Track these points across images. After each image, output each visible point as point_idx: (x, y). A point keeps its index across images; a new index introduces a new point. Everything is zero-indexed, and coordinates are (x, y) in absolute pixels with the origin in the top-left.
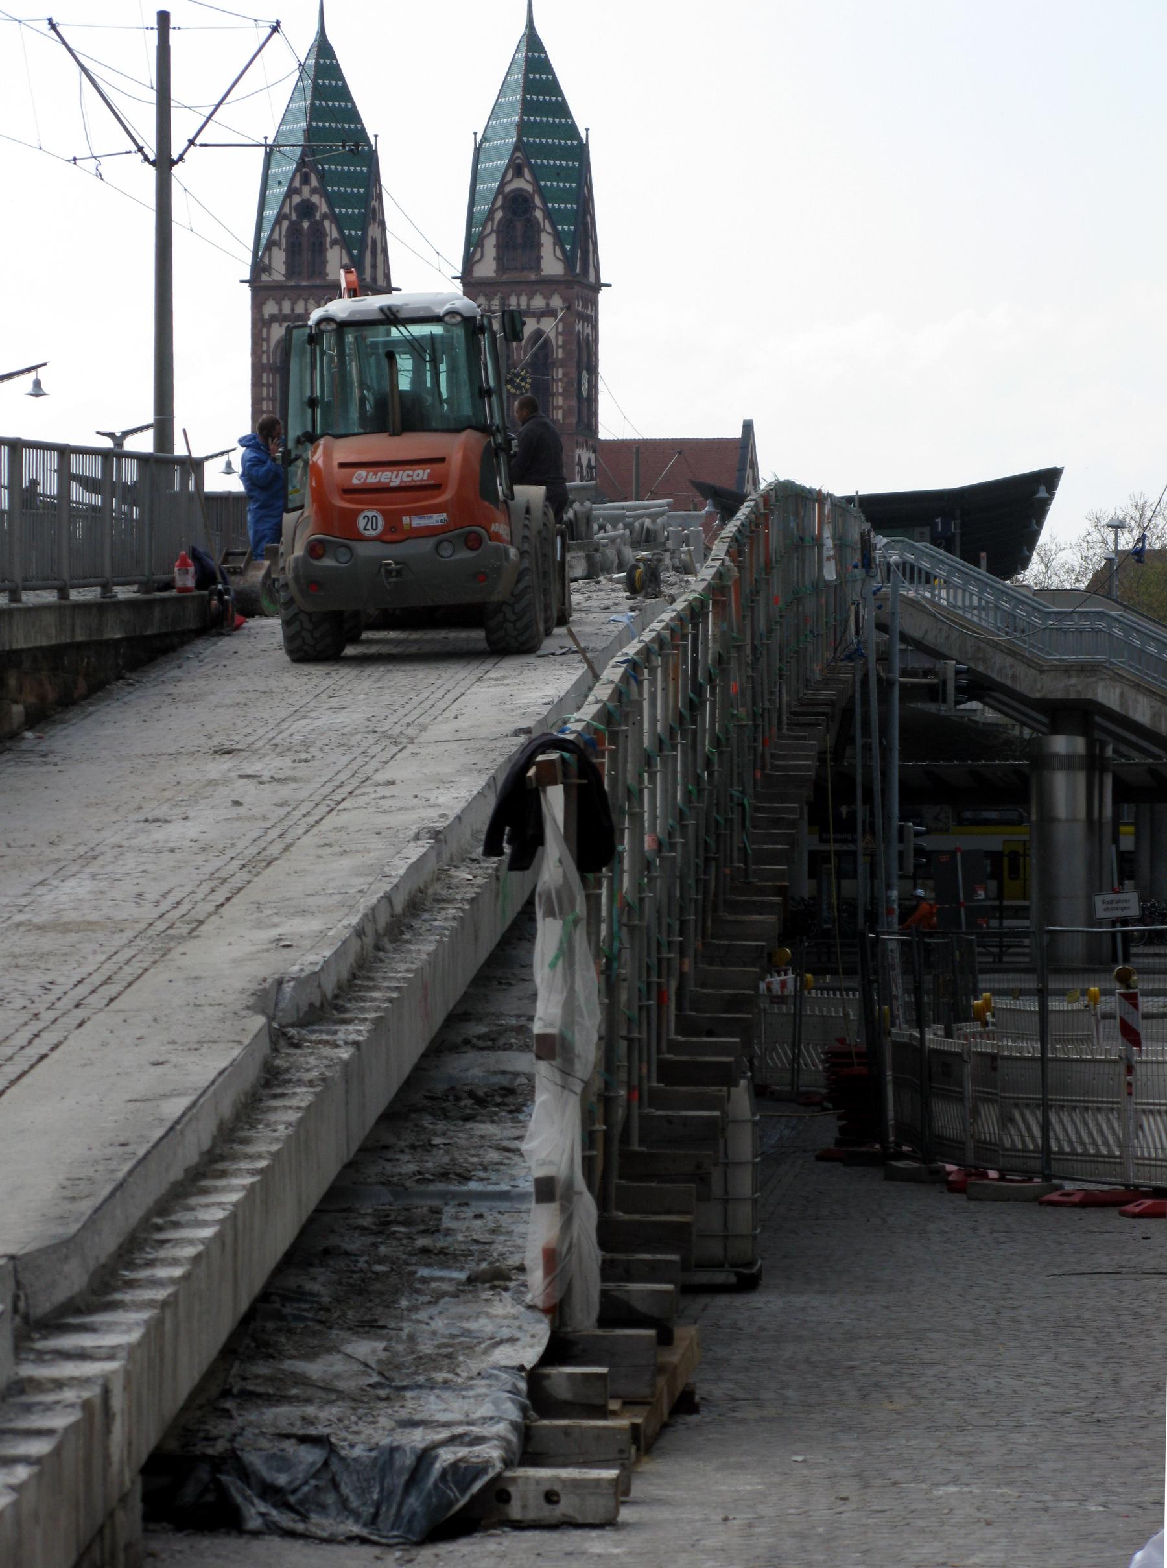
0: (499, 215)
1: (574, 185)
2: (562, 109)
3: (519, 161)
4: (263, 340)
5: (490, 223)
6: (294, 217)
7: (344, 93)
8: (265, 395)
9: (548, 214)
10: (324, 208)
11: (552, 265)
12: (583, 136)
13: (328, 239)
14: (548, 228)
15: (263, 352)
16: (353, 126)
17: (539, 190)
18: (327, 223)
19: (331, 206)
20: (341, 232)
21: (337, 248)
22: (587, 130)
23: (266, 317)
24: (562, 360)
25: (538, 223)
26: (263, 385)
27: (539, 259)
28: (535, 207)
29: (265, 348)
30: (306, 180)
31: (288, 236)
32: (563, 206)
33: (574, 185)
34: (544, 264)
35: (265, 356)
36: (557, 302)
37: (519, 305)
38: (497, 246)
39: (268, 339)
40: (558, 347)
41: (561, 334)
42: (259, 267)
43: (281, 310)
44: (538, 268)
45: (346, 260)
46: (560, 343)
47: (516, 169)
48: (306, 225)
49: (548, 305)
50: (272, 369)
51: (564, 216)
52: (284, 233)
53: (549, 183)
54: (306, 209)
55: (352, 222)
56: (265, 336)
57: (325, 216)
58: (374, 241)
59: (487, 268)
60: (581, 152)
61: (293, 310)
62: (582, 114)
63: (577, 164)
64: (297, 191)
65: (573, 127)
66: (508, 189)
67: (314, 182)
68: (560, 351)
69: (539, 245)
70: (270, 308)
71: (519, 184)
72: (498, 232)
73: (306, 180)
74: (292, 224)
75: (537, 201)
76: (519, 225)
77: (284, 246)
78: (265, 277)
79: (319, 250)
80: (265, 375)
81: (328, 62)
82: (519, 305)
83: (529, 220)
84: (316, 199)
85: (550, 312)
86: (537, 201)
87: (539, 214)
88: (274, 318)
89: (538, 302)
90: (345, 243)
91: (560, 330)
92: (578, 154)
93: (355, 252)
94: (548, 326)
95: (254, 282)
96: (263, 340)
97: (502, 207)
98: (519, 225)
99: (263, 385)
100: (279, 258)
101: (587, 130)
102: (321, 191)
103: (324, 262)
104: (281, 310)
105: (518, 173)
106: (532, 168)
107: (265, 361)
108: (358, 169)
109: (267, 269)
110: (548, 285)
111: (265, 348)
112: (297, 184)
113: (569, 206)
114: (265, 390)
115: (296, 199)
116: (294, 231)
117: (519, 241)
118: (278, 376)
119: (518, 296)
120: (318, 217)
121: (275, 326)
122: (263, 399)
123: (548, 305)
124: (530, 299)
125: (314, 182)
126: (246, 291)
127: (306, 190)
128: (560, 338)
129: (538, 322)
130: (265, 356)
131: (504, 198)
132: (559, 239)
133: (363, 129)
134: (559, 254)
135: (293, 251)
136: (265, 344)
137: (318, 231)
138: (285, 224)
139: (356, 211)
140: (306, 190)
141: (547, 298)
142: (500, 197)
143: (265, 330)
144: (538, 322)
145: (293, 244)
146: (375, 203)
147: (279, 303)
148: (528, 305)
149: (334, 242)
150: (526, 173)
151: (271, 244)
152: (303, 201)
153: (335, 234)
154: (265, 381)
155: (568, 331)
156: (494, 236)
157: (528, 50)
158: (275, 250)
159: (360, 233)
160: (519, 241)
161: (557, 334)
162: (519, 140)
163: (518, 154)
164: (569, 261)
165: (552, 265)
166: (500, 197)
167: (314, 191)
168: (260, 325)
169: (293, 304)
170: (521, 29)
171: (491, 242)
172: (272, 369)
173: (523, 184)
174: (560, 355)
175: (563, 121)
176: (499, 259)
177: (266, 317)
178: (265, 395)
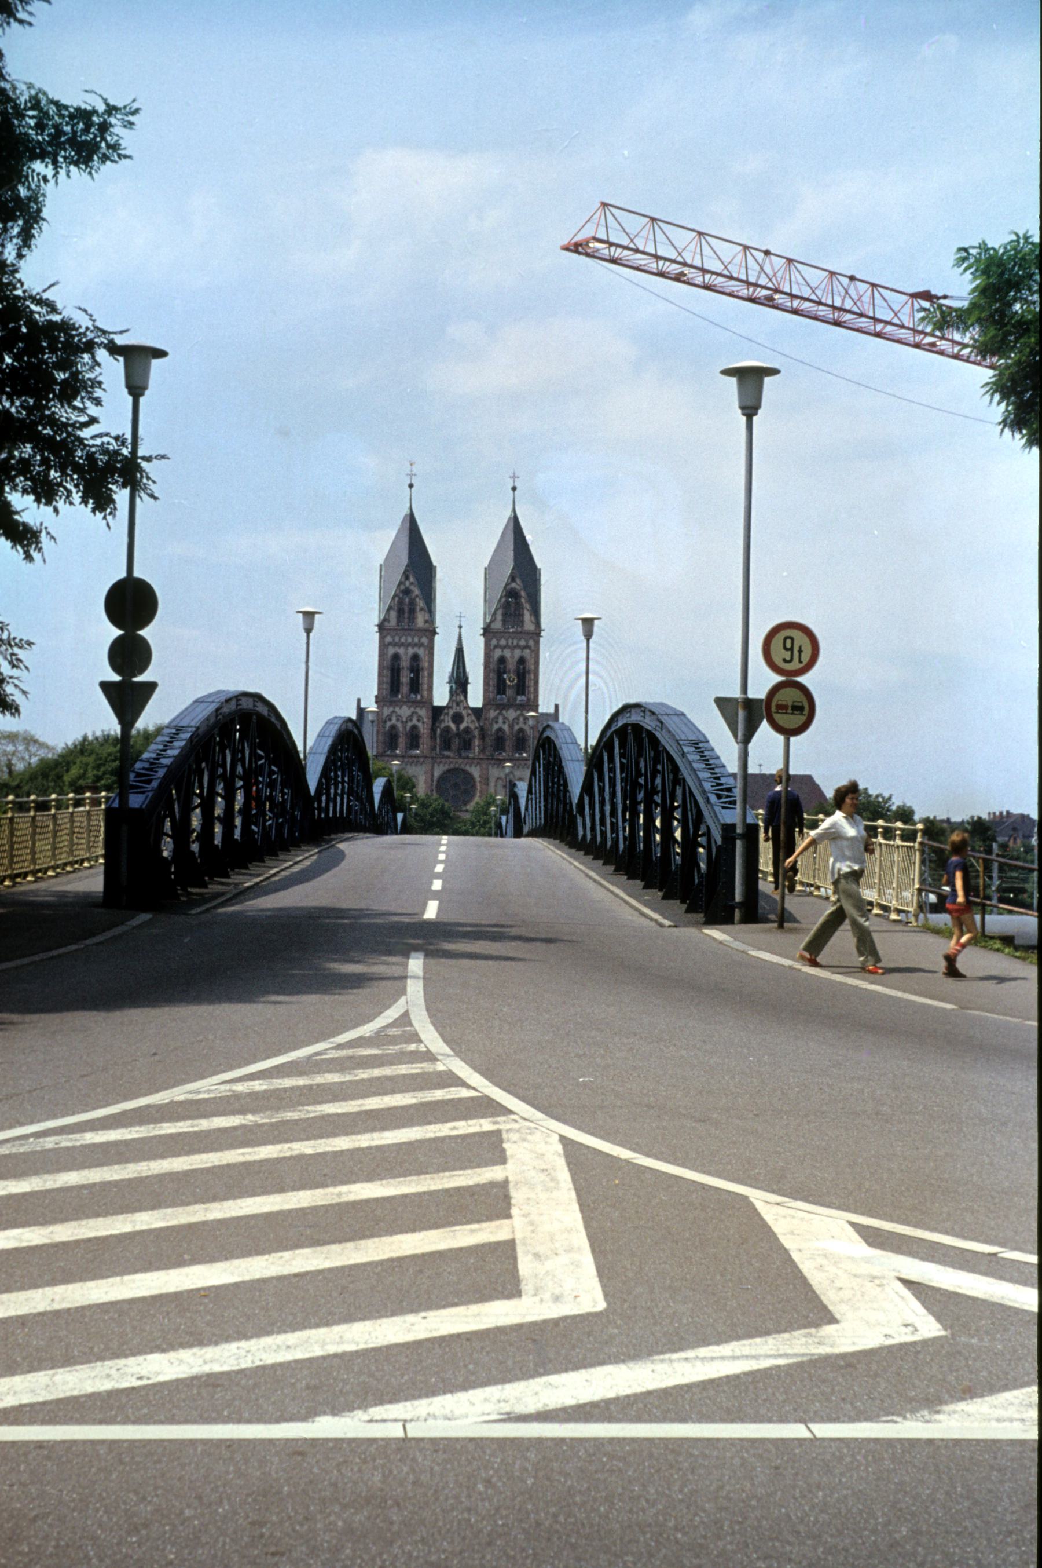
0: (503, 600)
13: (418, 608)
27: (523, 622)
30: (407, 578)
36: (531, 643)
44: (522, 626)
47: (513, 578)
48: (407, 600)
54: (407, 592)
66: (509, 587)
69: (523, 615)
70: (388, 639)
71: (513, 585)
73: (407, 578)
78: (386, 624)
79: (412, 611)
84: (412, 587)
87: (523, 600)
88: (390, 644)
89: (522, 643)
95: (381, 627)
100: (393, 614)
109: (389, 621)
110: (528, 633)
115: (402, 587)
116: (401, 602)
120: (413, 596)
125: (412, 579)
127: (407, 583)
135: (400, 612)
137: (412, 603)
140: (407, 583)
149: (422, 609)
150: (518, 581)
151: (390, 608)
165: (529, 626)
171: (500, 612)
173: (517, 585)
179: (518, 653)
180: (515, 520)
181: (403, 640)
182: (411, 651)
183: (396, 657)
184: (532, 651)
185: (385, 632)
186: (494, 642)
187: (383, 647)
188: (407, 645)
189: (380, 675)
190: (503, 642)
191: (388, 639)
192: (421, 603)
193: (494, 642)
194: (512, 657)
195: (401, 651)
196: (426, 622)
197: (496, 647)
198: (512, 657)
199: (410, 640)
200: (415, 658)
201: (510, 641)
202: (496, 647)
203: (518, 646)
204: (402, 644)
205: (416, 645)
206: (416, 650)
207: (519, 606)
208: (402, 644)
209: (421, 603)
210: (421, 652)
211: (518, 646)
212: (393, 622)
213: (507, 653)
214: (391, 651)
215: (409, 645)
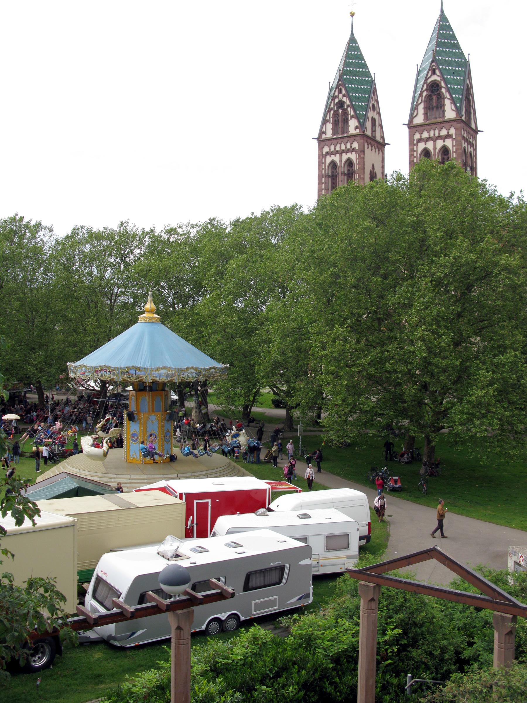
0: (425, 93)
1: (462, 78)
2: (457, 46)
3: (434, 67)
4: (323, 163)
5: (421, 98)
6: (336, 109)
7: (361, 57)
8: (323, 188)
9: (448, 90)
10: (348, 103)
11: (450, 113)
12: (467, 58)
13: (350, 116)
14: (448, 96)
15: (323, 169)
16: (364, 70)
17: (444, 79)
18: (349, 109)
19: (351, 101)
20: (355, 111)
21: (353, 119)
22: (469, 54)
23: (324, 153)
24: (456, 158)
25: (443, 94)
26: (323, 183)
27: (444, 111)
28: (442, 87)
29: (323, 167)
30: (340, 92)
31: (333, 117)
32: (456, 87)
34: (446, 114)
35: (323, 171)
36: (452, 131)
37: (434, 134)
38: (425, 108)
39: (325, 163)
40: (453, 152)
41: (455, 146)
42: (322, 133)
43: (330, 150)
44: (444, 116)
45: (357, 124)
46: (454, 150)
48: (340, 111)
49: (448, 133)
50: (328, 176)
51: (457, 91)
52: (331, 116)
53: (449, 77)
54: (341, 104)
55: (361, 108)
56: (323, 161)
57: (348, 106)
58: (373, 120)
59: (419, 119)
60: (466, 64)
61: (335, 149)
62: (467, 46)
63: (463, 69)
64: (337, 97)
65: (462, 54)
66: (429, 81)
67: (344, 92)
68: (454, 154)
69: (444, 105)
70: (326, 149)
71: (434, 78)
72: (425, 101)
73: (340, 92)
74: (335, 111)
75: (443, 84)
76: (434, 97)
77: (331, 122)
78: (324, 136)
79: (346, 122)
80: (323, 179)
81: (354, 45)
82: (434, 134)
83: (439, 94)
84: (345, 99)
85: (448, 136)
86: (443, 84)
87: (443, 90)
88: (327, 153)
89: (444, 132)
90: (357, 117)
91: (454, 144)
92: (463, 67)
93: (361, 120)
94: (449, 143)
96: (323, 163)
97: (426, 90)
98: (434, 97)
99: (323, 183)
100: (329, 127)
101: (469, 54)
102: (347, 95)
103: (349, 126)
104: (330, 150)
105: (434, 73)
107: (323, 173)
108: (366, 87)
109: (324, 133)
111: (323, 167)
112: (336, 94)
113: (459, 87)
114: (323, 185)
115: (337, 100)
116: (336, 114)
117: (435, 105)
118: (330, 179)
119: (434, 130)
122: (322, 189)
123: (448, 133)
124: (440, 131)
125: (344, 92)
126: (316, 142)
127: (340, 96)
128: (454, 148)
129: (444, 142)
130: (323, 171)
131: (427, 85)
132: (453, 101)
133: (369, 71)
134: (453, 108)
135: (335, 124)
136: (323, 165)
137: (345, 113)
138: (332, 112)
139: (363, 104)
141: (448, 129)
142: (425, 85)
143: (323, 159)
144: (444, 142)
145: (336, 121)
146: (372, 102)
147: (329, 147)
148: (439, 134)
149: (352, 117)
150: (437, 72)
153: (352, 113)
154: (323, 181)
155: (458, 144)
156: (423, 104)
157: (440, 21)
158: (328, 124)
159: (364, 113)
160: (435, 105)
161: (453, 146)
162: (434, 57)
163: (434, 64)
164: (458, 110)
165: (450, 113)
166: (425, 85)
167: (344, 96)
168: (321, 157)
169: (335, 146)
170: (437, 15)
171: (421, 107)
172: (328, 176)
174: (455, 156)
175: (457, 51)
176: (426, 114)
177: (324, 153)
178: (323, 188)
179: (440, 144)
180: (443, 18)
181: (338, 148)
182: (345, 157)
183: (333, 164)
184: (453, 139)
185: (323, 143)
186: (417, 136)
187: (322, 156)
188: (341, 152)
189: (320, 183)
190: (425, 135)
194: (435, 148)
195: (336, 158)
196: (356, 128)
197: (420, 140)
198: (435, 148)
199: (343, 147)
200: (350, 163)
201: (432, 133)
202: (420, 140)
203: (439, 137)
204: (337, 152)
205: (347, 151)
206: (349, 155)
207: (440, 97)
208: (337, 152)
209: (351, 112)
210: (353, 156)
211: (439, 137)
212: (329, 134)
213: (430, 145)
214: (329, 159)
215: (343, 151)
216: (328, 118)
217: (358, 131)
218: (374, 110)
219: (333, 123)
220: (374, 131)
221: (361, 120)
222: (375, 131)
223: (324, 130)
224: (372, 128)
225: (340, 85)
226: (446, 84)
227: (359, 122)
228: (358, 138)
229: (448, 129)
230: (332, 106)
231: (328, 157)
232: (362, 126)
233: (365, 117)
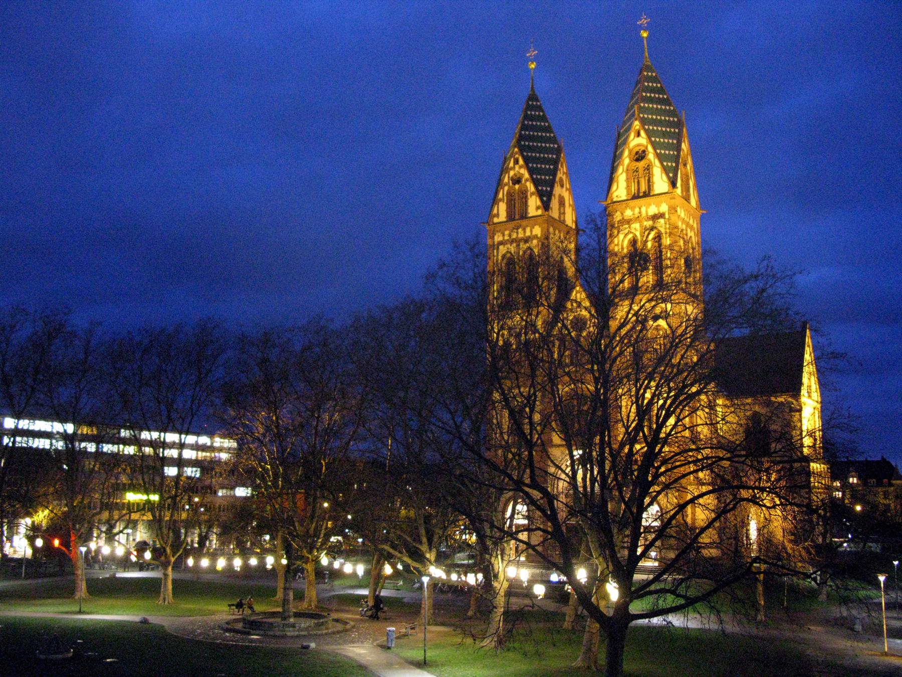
0: (627, 161)
10: (527, 175)
18: (528, 184)
20: (536, 186)
21: (534, 197)
30: (516, 162)
33: (675, 142)
38: (627, 179)
45: (539, 203)
57: (527, 180)
67: (521, 162)
73: (516, 162)
75: (650, 149)
88: (501, 243)
93: (545, 199)
106: (646, 131)
109: (498, 215)
115: (512, 173)
121: (501, 247)
127: (517, 166)
131: (630, 152)
132: (665, 170)
138: (506, 188)
141: (658, 206)
149: (532, 194)
150: (642, 133)
152: (515, 175)
167: (521, 167)
181: (514, 236)
182: (524, 246)
191: (498, 238)
192: (531, 187)
193: (618, 217)
196: (538, 208)
204: (512, 241)
216: (500, 196)
217: (540, 212)
218: (562, 186)
219: (507, 203)
220: (562, 213)
221: (545, 199)
222: (564, 213)
223: (495, 211)
224: (559, 210)
225: (516, 153)
226: (655, 149)
227: (542, 200)
228: (540, 220)
229: (658, 206)
230: (506, 180)
231: (501, 247)
232: (546, 206)
233: (550, 195)
